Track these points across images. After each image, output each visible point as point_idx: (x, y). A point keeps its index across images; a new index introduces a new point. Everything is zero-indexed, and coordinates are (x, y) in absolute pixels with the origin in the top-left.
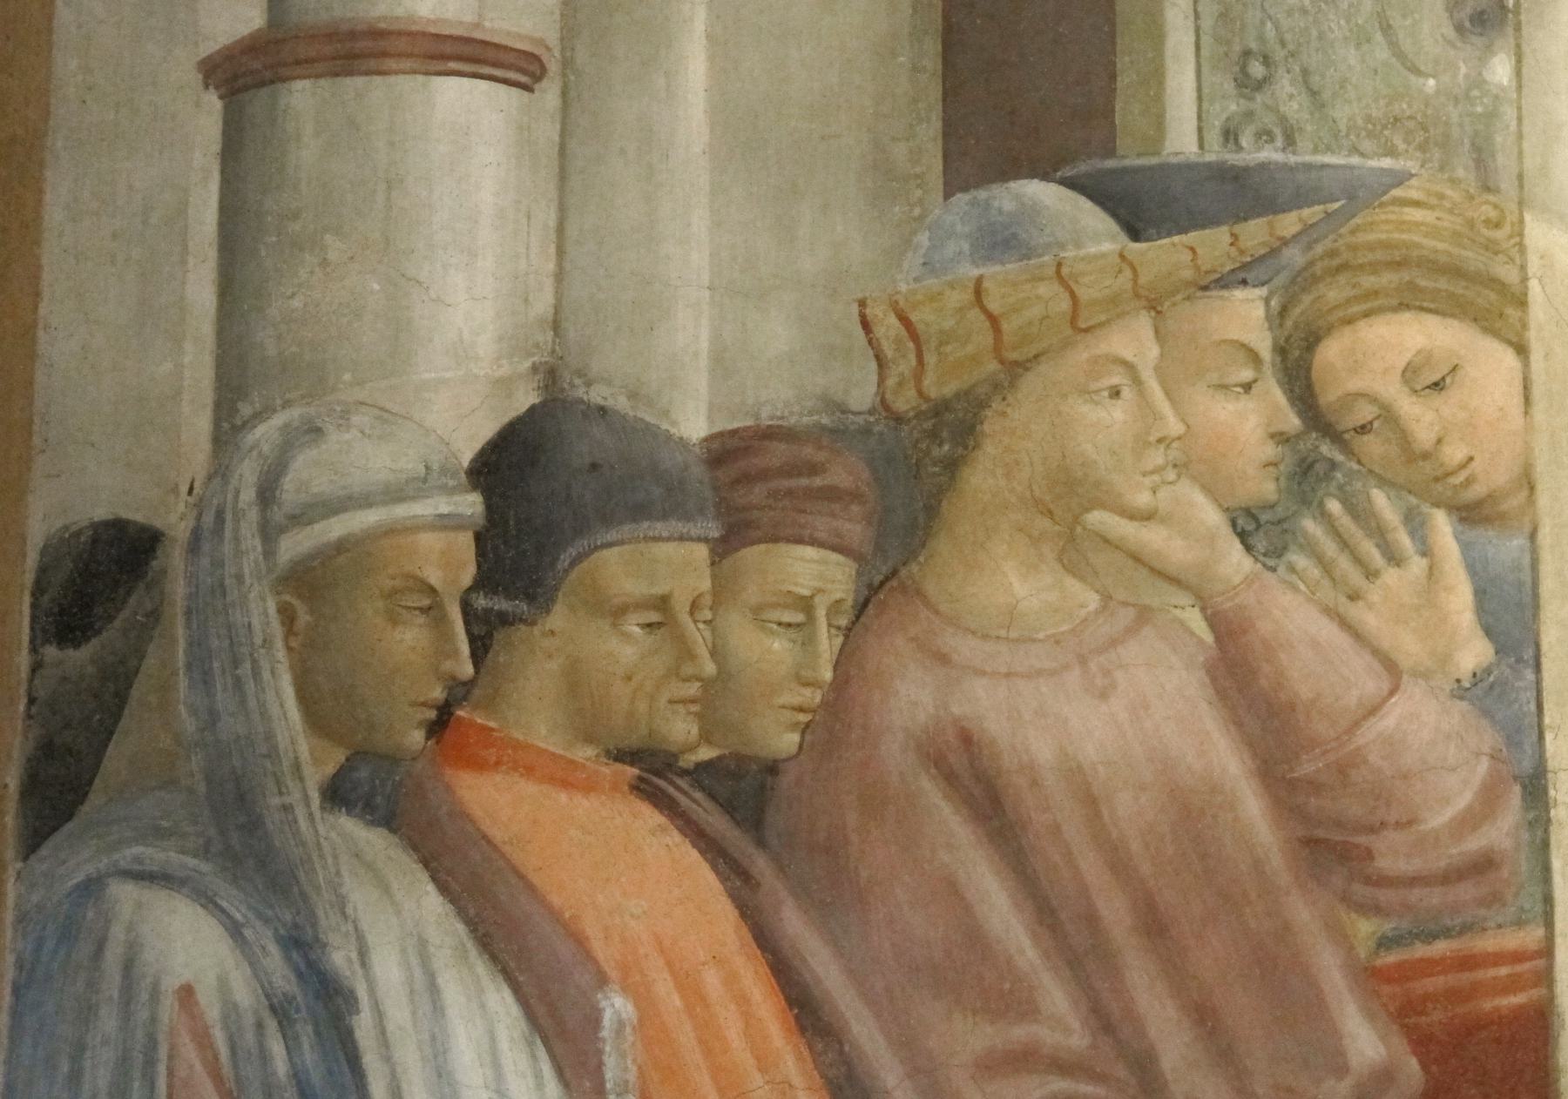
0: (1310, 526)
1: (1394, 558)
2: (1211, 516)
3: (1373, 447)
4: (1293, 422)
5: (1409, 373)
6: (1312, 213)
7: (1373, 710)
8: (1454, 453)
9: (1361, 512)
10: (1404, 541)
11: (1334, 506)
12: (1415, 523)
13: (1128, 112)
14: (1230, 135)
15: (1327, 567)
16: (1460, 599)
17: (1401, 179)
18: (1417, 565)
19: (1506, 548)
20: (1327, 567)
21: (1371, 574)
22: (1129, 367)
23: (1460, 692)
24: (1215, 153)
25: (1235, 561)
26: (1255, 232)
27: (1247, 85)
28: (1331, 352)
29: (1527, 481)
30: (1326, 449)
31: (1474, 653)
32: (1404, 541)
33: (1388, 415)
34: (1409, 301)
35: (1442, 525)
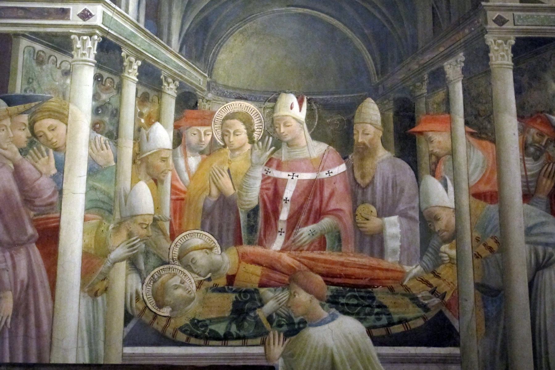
0: (31, 151)
1: (43, 156)
2: (16, 149)
3: (42, 139)
4: (30, 135)
5: (49, 128)
6: (37, 103)
7: (38, 179)
8: (54, 140)
9: (39, 150)
10: (45, 154)
11: (35, 148)
12: (47, 151)
13: (10, 87)
14: (25, 91)
15: (33, 158)
16: (53, 163)
17: (51, 97)
18: (47, 157)
19: (60, 155)
20: (33, 158)
21: (39, 159)
22: (6, 126)
23: (51, 177)
24: (23, 93)
25: (19, 156)
26: (27, 106)
27: (29, 83)
28: (37, 124)
29: (65, 145)
30: (35, 139)
31: (54, 171)
32: (45, 154)
33: (45, 134)
34: (50, 117)
35: (51, 152)
